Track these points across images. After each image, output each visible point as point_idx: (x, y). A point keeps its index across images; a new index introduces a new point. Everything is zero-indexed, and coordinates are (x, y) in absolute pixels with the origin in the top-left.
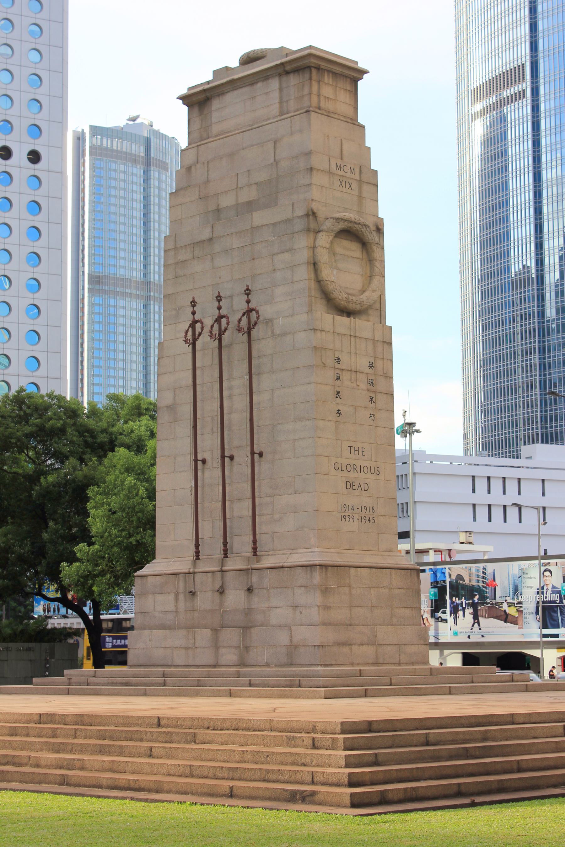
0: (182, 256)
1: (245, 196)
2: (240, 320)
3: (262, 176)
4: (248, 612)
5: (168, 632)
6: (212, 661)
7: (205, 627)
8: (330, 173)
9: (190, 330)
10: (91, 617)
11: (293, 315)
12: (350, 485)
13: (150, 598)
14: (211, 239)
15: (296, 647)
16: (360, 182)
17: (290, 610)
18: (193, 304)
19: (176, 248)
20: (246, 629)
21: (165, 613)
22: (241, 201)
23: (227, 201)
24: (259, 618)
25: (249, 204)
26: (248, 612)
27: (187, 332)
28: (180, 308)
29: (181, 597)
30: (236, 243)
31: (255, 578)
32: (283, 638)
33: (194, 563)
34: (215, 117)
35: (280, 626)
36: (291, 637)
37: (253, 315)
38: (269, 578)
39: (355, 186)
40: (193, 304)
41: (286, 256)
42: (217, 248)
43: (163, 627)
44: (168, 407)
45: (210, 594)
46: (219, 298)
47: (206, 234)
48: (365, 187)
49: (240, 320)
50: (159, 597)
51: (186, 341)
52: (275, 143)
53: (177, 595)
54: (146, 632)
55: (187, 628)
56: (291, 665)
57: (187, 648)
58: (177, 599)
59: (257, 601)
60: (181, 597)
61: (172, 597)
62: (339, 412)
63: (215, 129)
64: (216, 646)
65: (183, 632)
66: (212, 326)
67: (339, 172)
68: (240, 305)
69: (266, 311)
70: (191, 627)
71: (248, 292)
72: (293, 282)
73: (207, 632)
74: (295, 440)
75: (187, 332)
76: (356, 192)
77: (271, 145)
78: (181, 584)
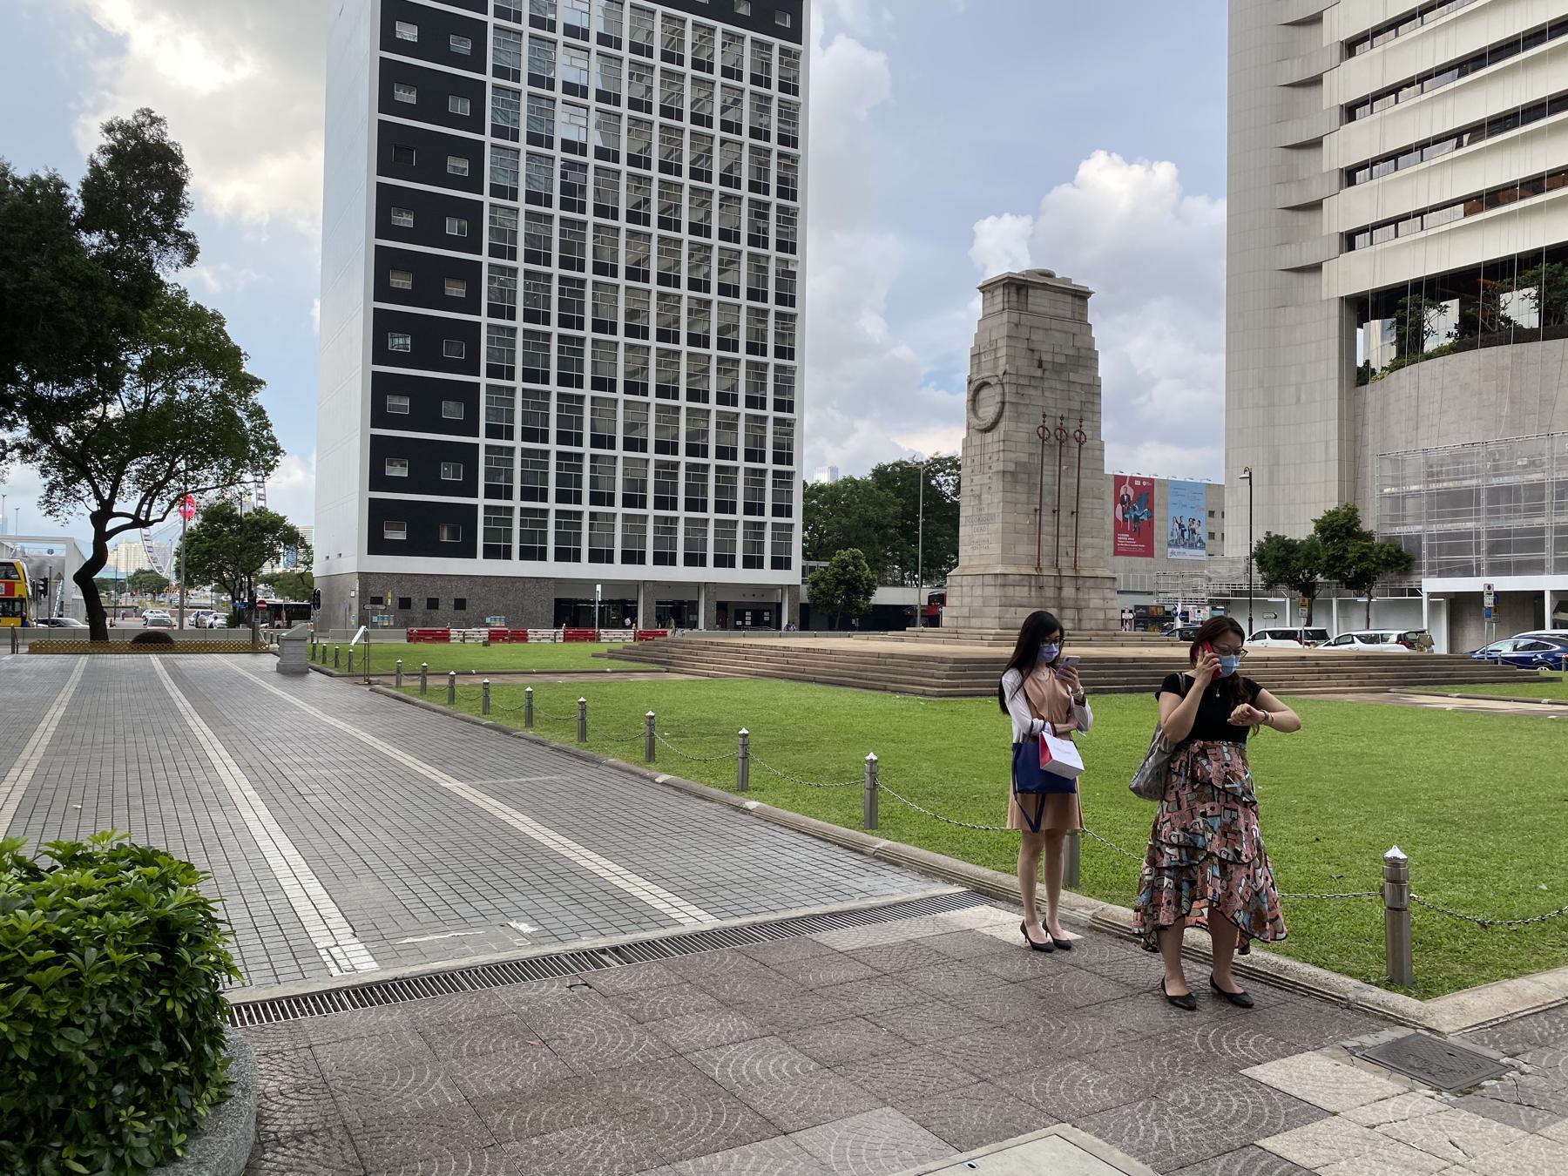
0: (1022, 381)
4: (1077, 600)
14: (1042, 378)
20: (1079, 609)
26: (1077, 600)
29: (1033, 589)
30: (1058, 386)
31: (1080, 582)
32: (1101, 615)
38: (1089, 583)
41: (1090, 406)
42: (1046, 384)
58: (1030, 590)
59: (1081, 595)
60: (1033, 589)
61: (1027, 588)
78: (1033, 583)
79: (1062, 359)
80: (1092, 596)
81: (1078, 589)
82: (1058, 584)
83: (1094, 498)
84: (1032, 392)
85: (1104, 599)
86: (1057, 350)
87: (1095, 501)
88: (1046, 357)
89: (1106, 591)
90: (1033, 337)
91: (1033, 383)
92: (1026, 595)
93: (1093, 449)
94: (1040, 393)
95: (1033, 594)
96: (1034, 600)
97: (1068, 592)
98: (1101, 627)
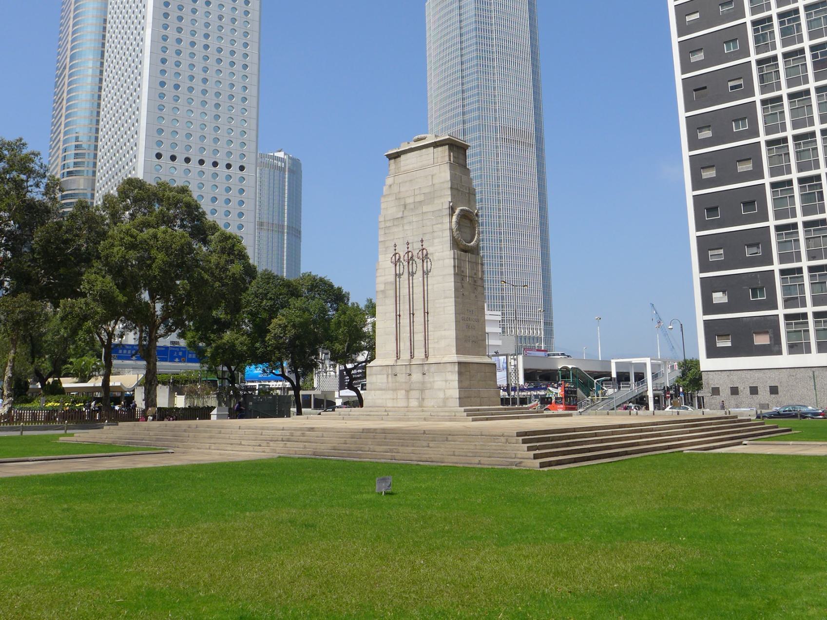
0: (388, 224)
1: (418, 199)
2: (418, 254)
3: (427, 190)
4: (423, 383)
5: (383, 392)
6: (405, 405)
7: (402, 389)
8: (457, 189)
9: (394, 257)
10: (295, 384)
11: (443, 252)
12: (468, 327)
13: (375, 376)
14: (402, 217)
15: (447, 399)
16: (469, 193)
17: (444, 382)
18: (395, 246)
19: (385, 221)
20: (422, 391)
21: (382, 383)
22: (416, 201)
23: (410, 200)
24: (429, 385)
25: (420, 202)
26: (423, 383)
27: (392, 258)
28: (387, 247)
29: (390, 376)
31: (426, 367)
32: (441, 395)
33: (396, 361)
34: (402, 163)
35: (440, 389)
36: (445, 394)
37: (425, 251)
38: (433, 368)
39: (467, 195)
40: (395, 246)
41: (439, 226)
42: (405, 221)
43: (381, 390)
44: (382, 291)
45: (404, 375)
46: (408, 244)
47: (400, 215)
48: (472, 196)
49: (418, 254)
50: (379, 376)
51: (392, 262)
52: (432, 176)
53: (388, 376)
54: (373, 392)
55: (393, 390)
56: (445, 406)
57: (393, 399)
58: (388, 377)
59: (426, 377)
60: (390, 376)
61: (385, 376)
62: (463, 294)
63: (402, 169)
64: (408, 398)
65: (391, 392)
66: (404, 256)
67: (462, 190)
68: (418, 246)
69: (430, 250)
70: (395, 390)
71: (422, 241)
72: (443, 237)
73: (403, 392)
74: (444, 307)
75: (392, 258)
76: (468, 198)
77: (431, 177)
79: (421, 198)
80: (436, 379)
81: (424, 374)
82: (408, 372)
83: (445, 298)
84: (395, 230)
85: (446, 381)
86: (417, 192)
87: (446, 300)
88: (410, 200)
89: (447, 374)
90: (402, 189)
91: (395, 223)
92: (385, 381)
93: (443, 260)
94: (401, 228)
95: (390, 379)
96: (390, 385)
97: (416, 376)
98: (441, 404)
